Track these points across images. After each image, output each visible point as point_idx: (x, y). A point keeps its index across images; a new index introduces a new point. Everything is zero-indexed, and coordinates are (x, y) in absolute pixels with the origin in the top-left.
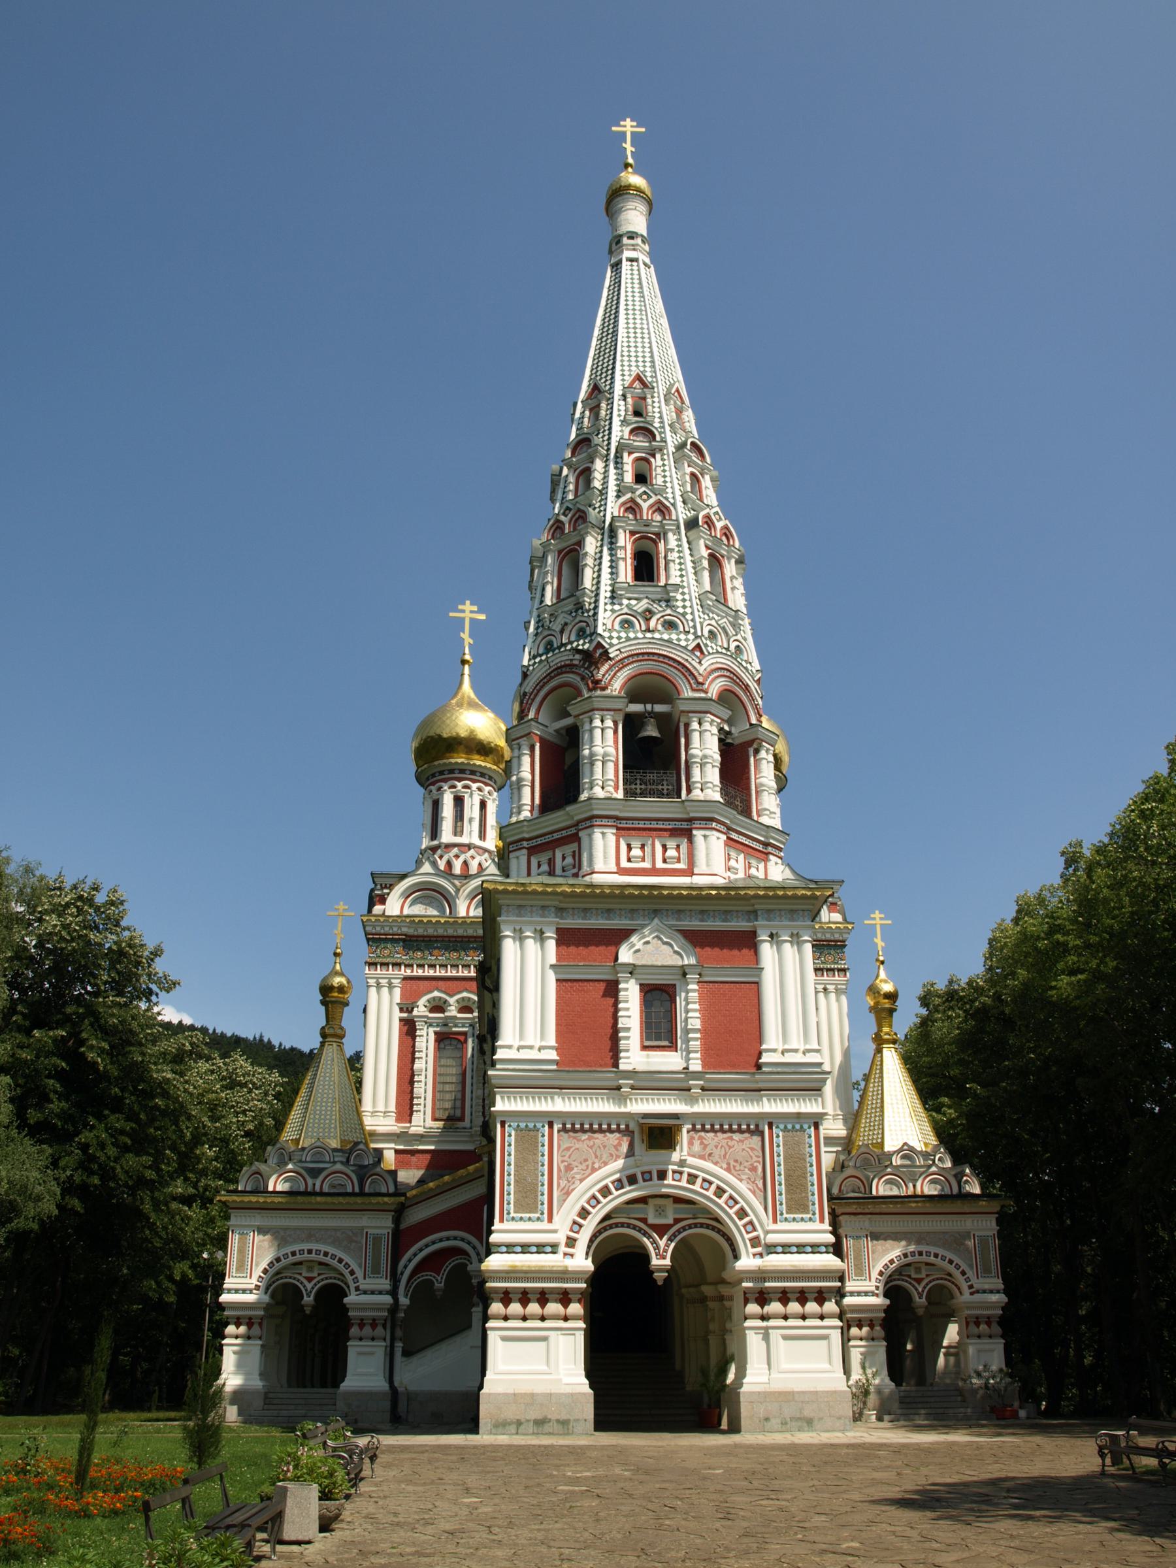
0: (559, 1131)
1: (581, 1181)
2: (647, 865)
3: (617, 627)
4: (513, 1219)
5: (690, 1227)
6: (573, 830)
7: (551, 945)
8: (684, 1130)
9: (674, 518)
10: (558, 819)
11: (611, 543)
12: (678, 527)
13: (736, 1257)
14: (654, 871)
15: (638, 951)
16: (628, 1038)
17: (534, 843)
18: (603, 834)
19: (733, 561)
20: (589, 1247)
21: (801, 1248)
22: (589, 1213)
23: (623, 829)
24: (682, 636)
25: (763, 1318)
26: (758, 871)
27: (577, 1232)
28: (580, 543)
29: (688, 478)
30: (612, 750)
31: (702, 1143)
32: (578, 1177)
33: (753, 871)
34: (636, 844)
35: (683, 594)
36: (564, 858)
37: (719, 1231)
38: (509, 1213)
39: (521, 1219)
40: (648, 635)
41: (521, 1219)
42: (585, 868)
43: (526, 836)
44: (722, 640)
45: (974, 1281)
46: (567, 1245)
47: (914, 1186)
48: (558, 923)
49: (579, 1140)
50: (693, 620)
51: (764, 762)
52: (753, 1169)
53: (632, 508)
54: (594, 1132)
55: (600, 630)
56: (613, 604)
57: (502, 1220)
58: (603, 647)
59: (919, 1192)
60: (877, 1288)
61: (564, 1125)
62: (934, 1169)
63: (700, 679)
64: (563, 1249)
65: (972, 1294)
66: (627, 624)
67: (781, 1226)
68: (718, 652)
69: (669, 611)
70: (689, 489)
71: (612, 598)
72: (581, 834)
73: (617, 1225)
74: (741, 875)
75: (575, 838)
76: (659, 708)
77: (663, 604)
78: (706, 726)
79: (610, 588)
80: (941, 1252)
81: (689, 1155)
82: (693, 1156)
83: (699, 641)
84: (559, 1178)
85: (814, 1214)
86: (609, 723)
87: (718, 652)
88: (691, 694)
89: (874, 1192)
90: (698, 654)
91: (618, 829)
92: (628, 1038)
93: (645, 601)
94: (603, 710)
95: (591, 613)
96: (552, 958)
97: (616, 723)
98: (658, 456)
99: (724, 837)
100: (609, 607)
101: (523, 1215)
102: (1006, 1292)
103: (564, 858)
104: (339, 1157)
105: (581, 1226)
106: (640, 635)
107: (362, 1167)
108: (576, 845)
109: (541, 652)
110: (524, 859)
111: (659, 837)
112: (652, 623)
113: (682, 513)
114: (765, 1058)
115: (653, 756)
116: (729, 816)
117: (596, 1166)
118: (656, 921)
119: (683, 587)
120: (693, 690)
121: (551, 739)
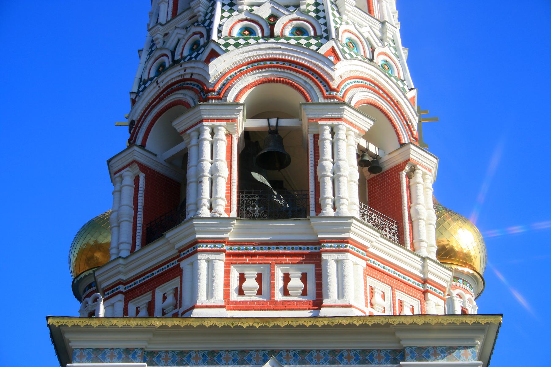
3: (235, 33)
6: (175, 263)
17: (132, 285)
24: (313, 41)
34: (251, 274)
36: (164, 298)
40: (272, 40)
42: (186, 303)
43: (124, 278)
50: (325, 24)
55: (214, 37)
56: (231, 11)
63: (334, 85)
75: (177, 272)
76: (285, 122)
88: (321, 100)
91: (229, 255)
94: (212, 120)
95: (208, 22)
97: (229, 135)
99: (363, 263)
103: (164, 298)
106: (261, 41)
108: (178, 279)
109: (152, 75)
111: (280, 263)
120: (325, 97)
121: (158, 169)
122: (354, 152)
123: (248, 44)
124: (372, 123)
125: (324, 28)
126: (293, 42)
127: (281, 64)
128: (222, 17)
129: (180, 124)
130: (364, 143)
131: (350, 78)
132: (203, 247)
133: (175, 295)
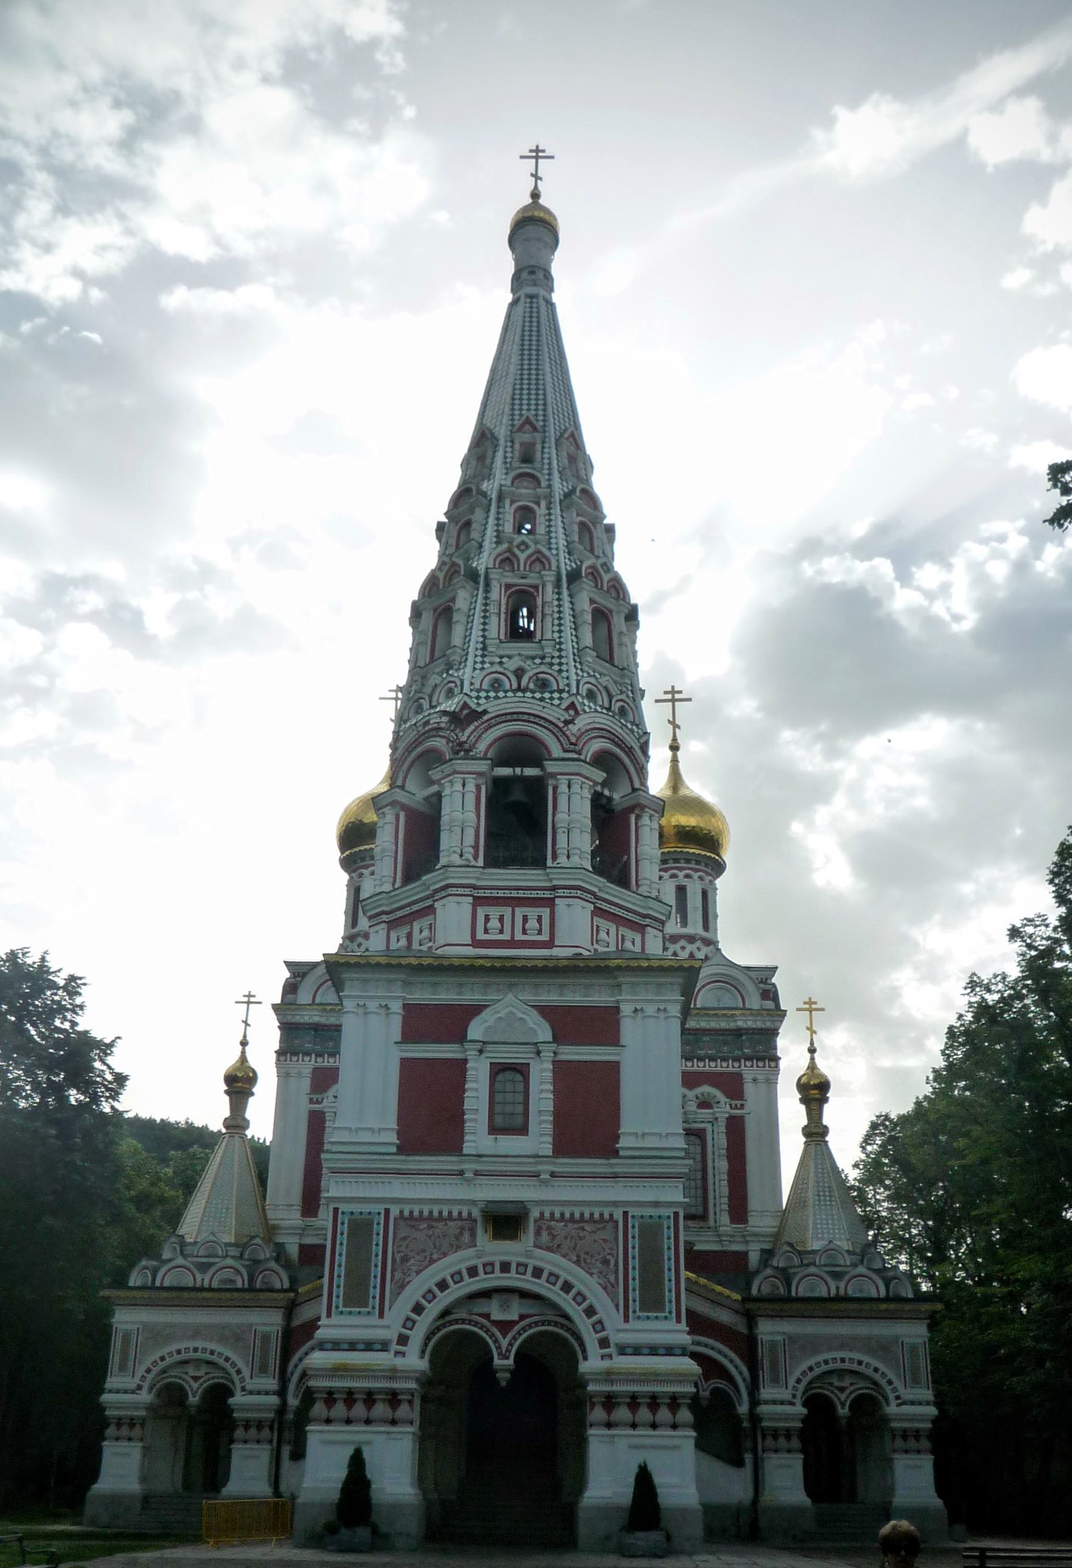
0: (395, 1219)
1: (418, 1273)
2: (505, 936)
3: (485, 686)
4: (341, 1313)
5: (536, 1323)
7: (397, 1023)
8: (532, 1220)
9: (554, 567)
10: (415, 891)
11: (486, 598)
12: (559, 579)
13: (585, 1358)
14: (512, 944)
15: (490, 1027)
16: (475, 1120)
18: (458, 903)
19: (623, 615)
20: (426, 1345)
21: (653, 1350)
22: (423, 1309)
23: (479, 897)
24: (556, 695)
25: (609, 1425)
26: (632, 942)
27: (411, 1329)
28: (453, 600)
29: (576, 528)
30: (472, 816)
31: (550, 1234)
32: (414, 1268)
33: (628, 945)
35: (560, 650)
37: (568, 1330)
38: (337, 1307)
39: (350, 1313)
40: (520, 694)
41: (350, 1313)
44: (602, 699)
45: (901, 1391)
46: (398, 1344)
47: (838, 1288)
48: (404, 998)
49: (418, 1230)
50: (567, 678)
51: (647, 829)
52: (606, 1262)
53: (507, 561)
54: (436, 1220)
55: (466, 690)
57: (329, 1315)
58: (470, 708)
59: (842, 1292)
60: (794, 1396)
61: (401, 1212)
62: (861, 1269)
63: (573, 740)
64: (394, 1347)
65: (899, 1405)
66: (496, 685)
67: (633, 1324)
68: (596, 711)
69: (543, 668)
70: (576, 538)
71: (483, 656)
72: (436, 905)
73: (457, 1321)
74: (612, 948)
75: (430, 910)
76: (530, 772)
77: (538, 661)
78: (576, 788)
79: (480, 646)
80: (866, 1359)
81: (535, 1246)
82: (540, 1248)
83: (573, 699)
84: (393, 1270)
85: (670, 1312)
86: (471, 787)
87: (596, 711)
89: (793, 1294)
90: (572, 712)
92: (475, 1120)
93: (517, 658)
96: (396, 1034)
97: (478, 787)
98: (543, 504)
100: (478, 666)
101: (353, 1309)
102: (936, 1404)
104: (234, 1252)
105: (414, 1322)
106: (510, 694)
107: (257, 1262)
108: (432, 917)
110: (383, 934)
112: (524, 681)
113: (565, 565)
114: (623, 1143)
115: (517, 821)
116: (598, 884)
117: (435, 1256)
118: (510, 996)
119: (560, 643)
121: (414, 805)
122: (587, 795)
123: (497, 698)
124: (605, 775)
125: (566, 681)
126: (538, 695)
127: (526, 717)
128: (475, 669)
129: (435, 774)
130: (599, 788)
131: (588, 731)
132: (454, 891)
133: (430, 928)
